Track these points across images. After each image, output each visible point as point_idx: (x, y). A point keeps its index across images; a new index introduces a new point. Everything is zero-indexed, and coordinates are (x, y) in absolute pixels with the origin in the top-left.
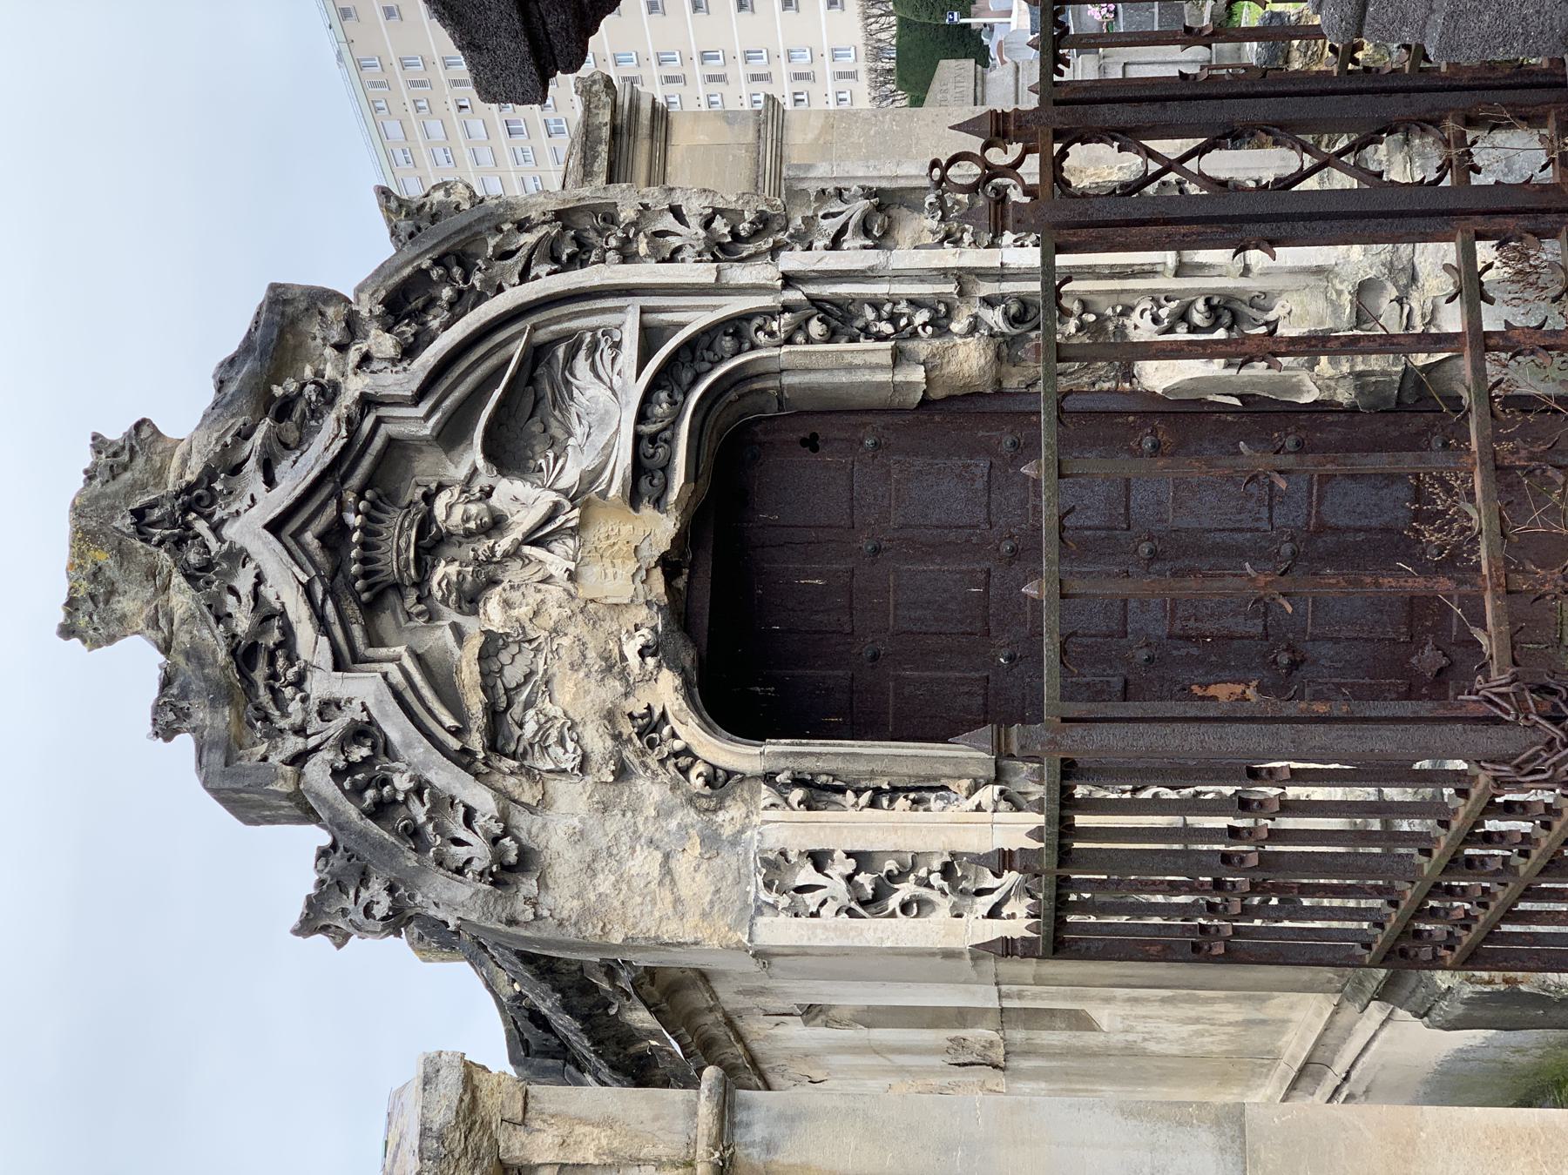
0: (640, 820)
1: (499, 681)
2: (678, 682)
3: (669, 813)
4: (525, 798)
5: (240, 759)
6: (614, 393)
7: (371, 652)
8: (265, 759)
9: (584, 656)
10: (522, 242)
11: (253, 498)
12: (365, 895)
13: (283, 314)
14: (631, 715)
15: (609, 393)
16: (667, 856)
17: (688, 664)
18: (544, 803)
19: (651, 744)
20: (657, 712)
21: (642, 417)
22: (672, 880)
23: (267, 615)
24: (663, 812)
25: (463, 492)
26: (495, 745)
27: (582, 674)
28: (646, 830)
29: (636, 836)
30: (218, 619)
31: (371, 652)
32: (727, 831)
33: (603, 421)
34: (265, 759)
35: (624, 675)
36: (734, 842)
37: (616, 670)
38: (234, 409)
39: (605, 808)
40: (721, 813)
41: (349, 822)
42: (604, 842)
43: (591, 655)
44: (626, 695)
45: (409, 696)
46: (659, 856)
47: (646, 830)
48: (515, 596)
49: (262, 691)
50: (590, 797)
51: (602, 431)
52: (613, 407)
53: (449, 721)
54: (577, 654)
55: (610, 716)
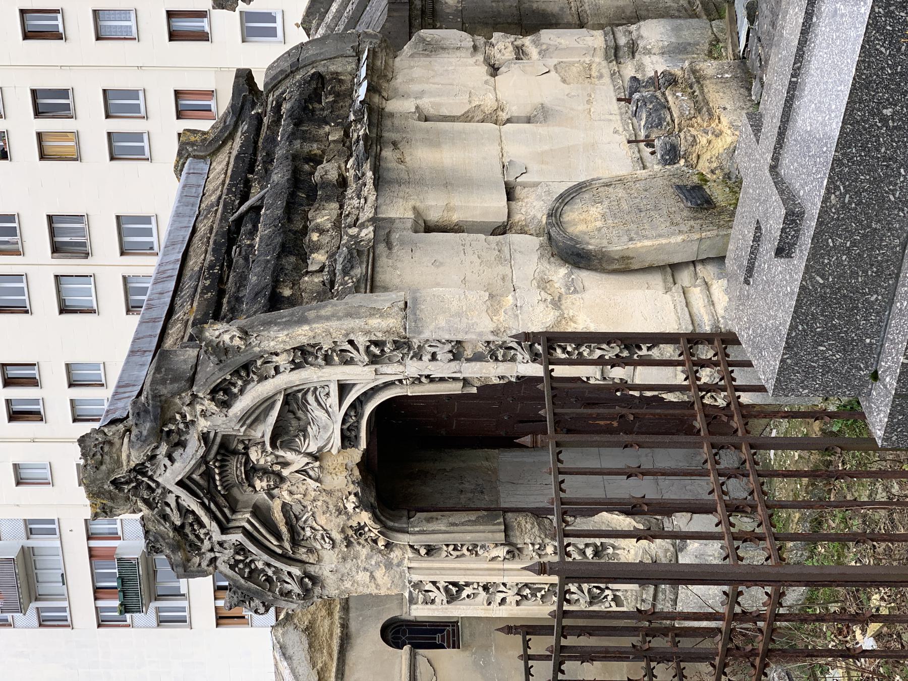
0: (359, 561)
1: (291, 512)
2: (370, 515)
3: (371, 557)
4: (311, 561)
5: (190, 567)
6: (329, 415)
7: (234, 517)
8: (200, 565)
9: (328, 508)
10: (274, 360)
11: (165, 466)
12: (252, 604)
13: (160, 401)
14: (351, 527)
15: (326, 415)
16: (371, 573)
17: (372, 500)
18: (319, 560)
19: (361, 535)
20: (362, 524)
21: (344, 421)
22: (375, 579)
23: (184, 512)
24: (369, 557)
25: (262, 453)
26: (296, 541)
27: (328, 515)
28: (362, 565)
29: (358, 567)
30: (165, 520)
31: (234, 517)
32: (395, 561)
33: (325, 428)
34: (200, 565)
35: (347, 513)
36: (398, 565)
37: (343, 512)
38: (148, 442)
39: (344, 559)
40: (392, 553)
41: (241, 585)
42: (346, 571)
43: (331, 507)
44: (348, 519)
45: (256, 534)
46: (368, 574)
47: (362, 565)
48: (294, 489)
49: (190, 535)
50: (338, 555)
51: (326, 432)
52: (329, 422)
53: (276, 543)
54: (325, 508)
55: (343, 531)
